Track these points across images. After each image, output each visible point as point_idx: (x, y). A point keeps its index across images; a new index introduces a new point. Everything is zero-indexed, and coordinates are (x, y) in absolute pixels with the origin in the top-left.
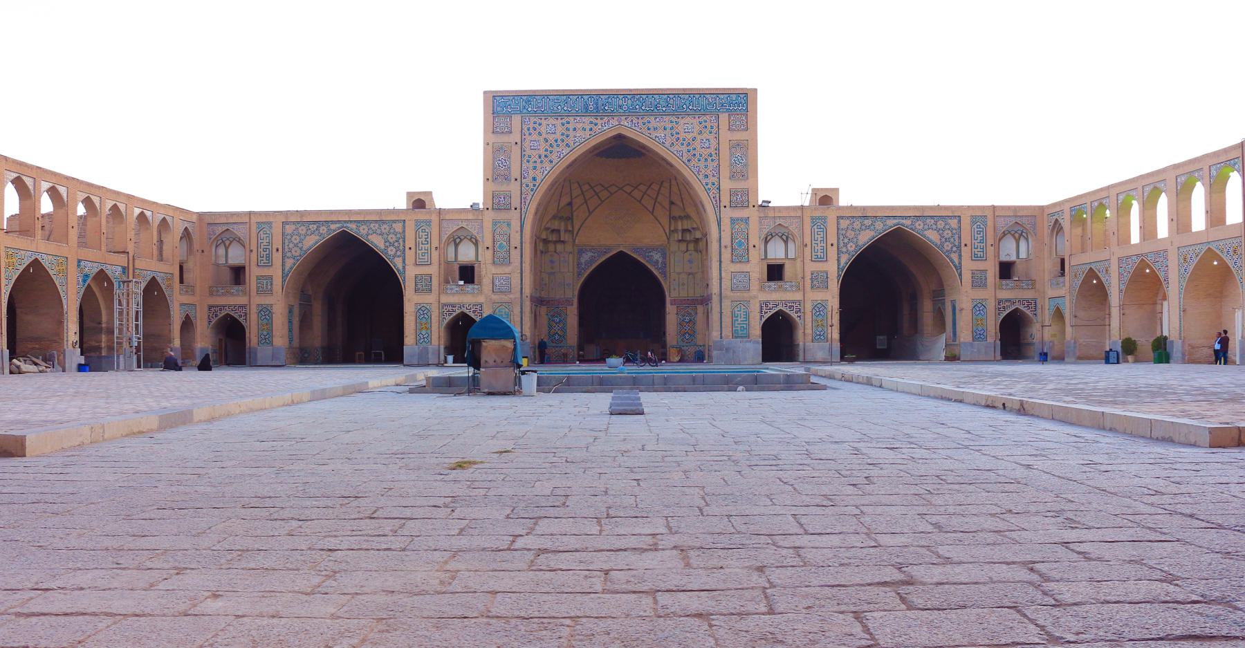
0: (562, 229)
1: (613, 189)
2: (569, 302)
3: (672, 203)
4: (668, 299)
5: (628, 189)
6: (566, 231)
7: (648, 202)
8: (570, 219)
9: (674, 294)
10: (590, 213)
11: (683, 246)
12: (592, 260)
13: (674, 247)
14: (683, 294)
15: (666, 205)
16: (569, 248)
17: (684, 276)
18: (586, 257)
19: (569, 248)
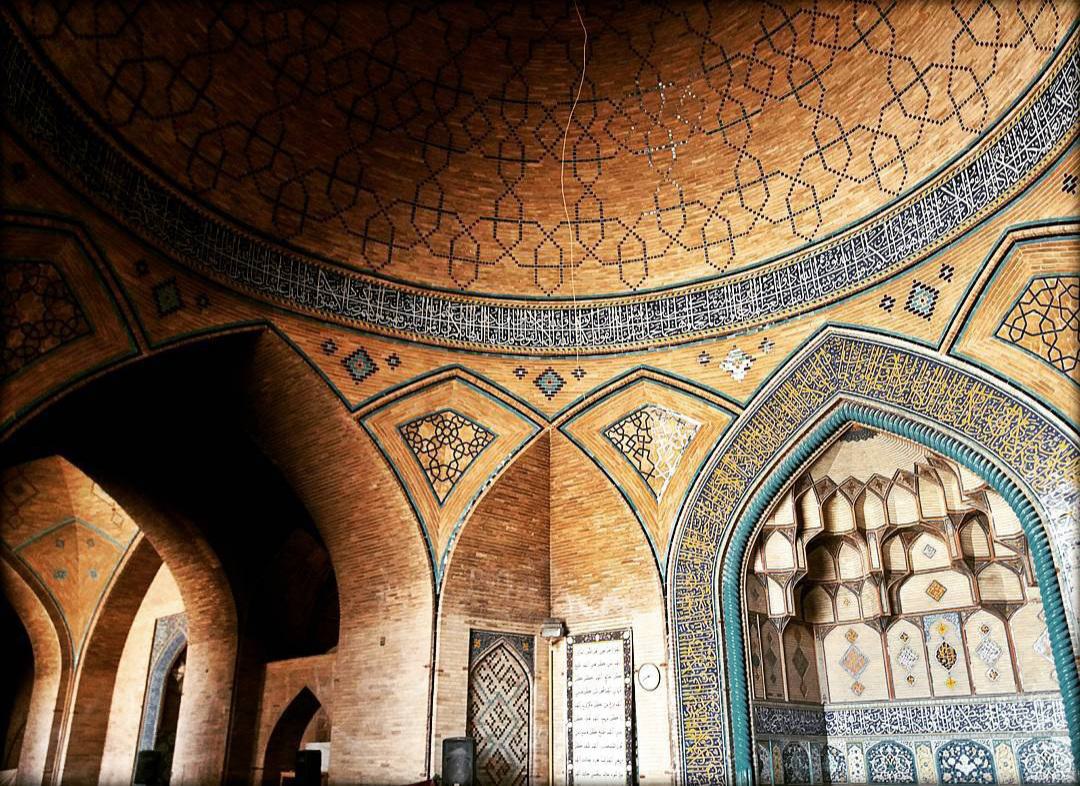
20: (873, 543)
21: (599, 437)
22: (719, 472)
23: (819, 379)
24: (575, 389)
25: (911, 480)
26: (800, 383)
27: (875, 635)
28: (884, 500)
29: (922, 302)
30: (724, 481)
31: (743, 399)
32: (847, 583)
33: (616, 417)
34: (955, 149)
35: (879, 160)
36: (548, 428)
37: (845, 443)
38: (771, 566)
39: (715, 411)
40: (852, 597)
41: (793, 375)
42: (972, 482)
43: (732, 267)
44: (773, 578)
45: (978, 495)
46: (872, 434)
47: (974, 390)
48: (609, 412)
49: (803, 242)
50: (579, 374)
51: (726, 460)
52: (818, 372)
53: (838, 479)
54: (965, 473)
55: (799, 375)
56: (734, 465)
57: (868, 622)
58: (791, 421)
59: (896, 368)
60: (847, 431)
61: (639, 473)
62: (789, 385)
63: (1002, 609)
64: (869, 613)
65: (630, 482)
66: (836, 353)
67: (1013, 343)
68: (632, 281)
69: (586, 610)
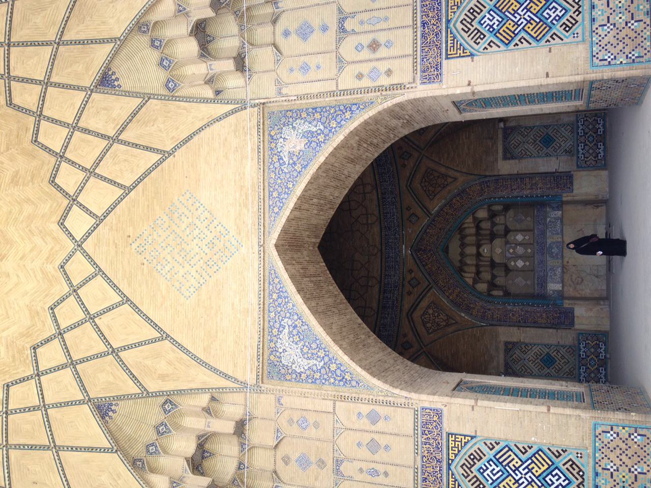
0: (197, 424)
1: (79, 268)
2: (429, 422)
3: (106, 81)
4: (423, 91)
5: (79, 223)
6: (207, 411)
7: (125, 165)
8: (169, 401)
9: (404, 71)
10: (165, 336)
11: (261, 58)
12: (300, 334)
13: (262, 87)
14: (404, 41)
15: (122, 107)
16: (264, 404)
17: (348, 49)
18: (292, 354)
19: (264, 404)
20: (480, 263)
21: (431, 335)
22: (451, 298)
23: (427, 256)
24: (411, 337)
25: (463, 245)
26: (426, 263)
27: (511, 273)
28: (467, 256)
29: (414, 219)
30: (454, 295)
31: (427, 283)
32: (492, 278)
33: (424, 329)
34: (375, 197)
35: (365, 222)
36: (425, 349)
37: (450, 255)
38: (486, 291)
39: (429, 294)
40: (498, 279)
41: (423, 265)
42: (470, 219)
43: (379, 278)
44: (491, 291)
45: (475, 219)
46: (448, 246)
47: (444, 209)
48: (421, 330)
49: (379, 254)
50: (405, 336)
51: (447, 294)
52: (425, 256)
53: (458, 264)
54: (468, 221)
55: (424, 263)
56: (450, 291)
57: (506, 276)
58: (439, 268)
59: (431, 231)
60: (446, 250)
61: (446, 326)
62: (426, 267)
63: (507, 231)
64: (503, 274)
65: (450, 329)
66: (421, 249)
67: (435, 196)
68: (372, 313)
69: (495, 364)
